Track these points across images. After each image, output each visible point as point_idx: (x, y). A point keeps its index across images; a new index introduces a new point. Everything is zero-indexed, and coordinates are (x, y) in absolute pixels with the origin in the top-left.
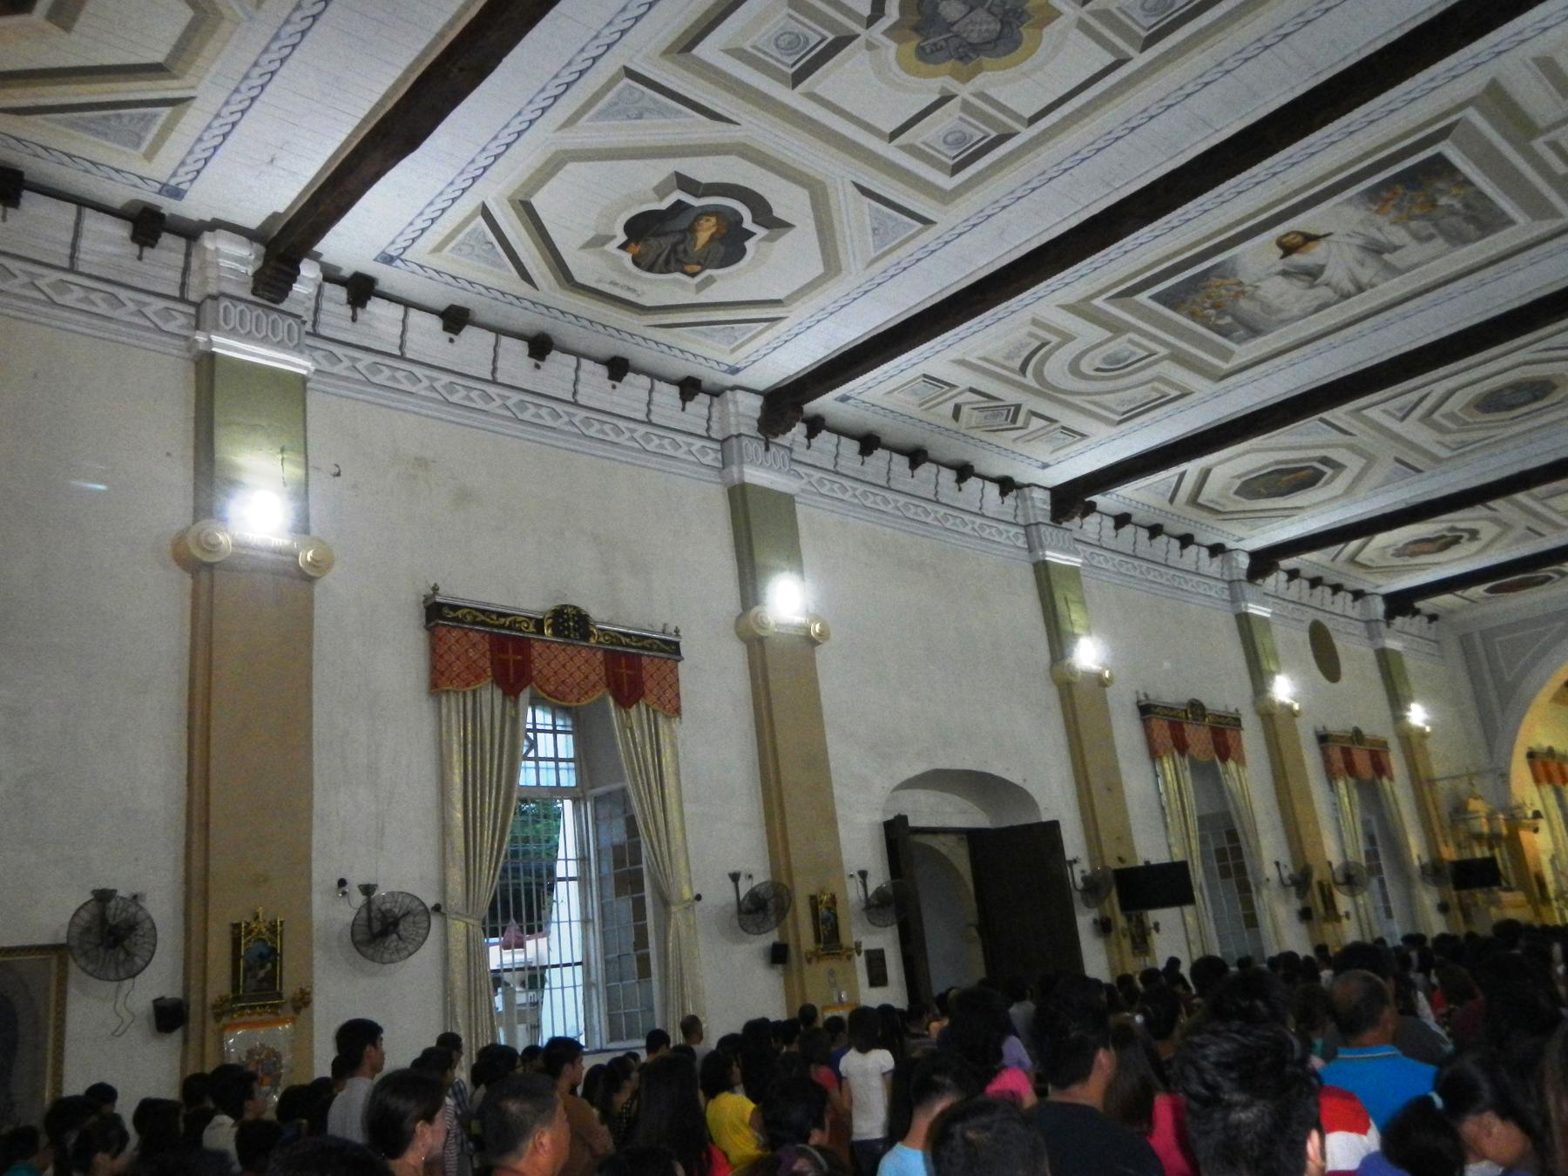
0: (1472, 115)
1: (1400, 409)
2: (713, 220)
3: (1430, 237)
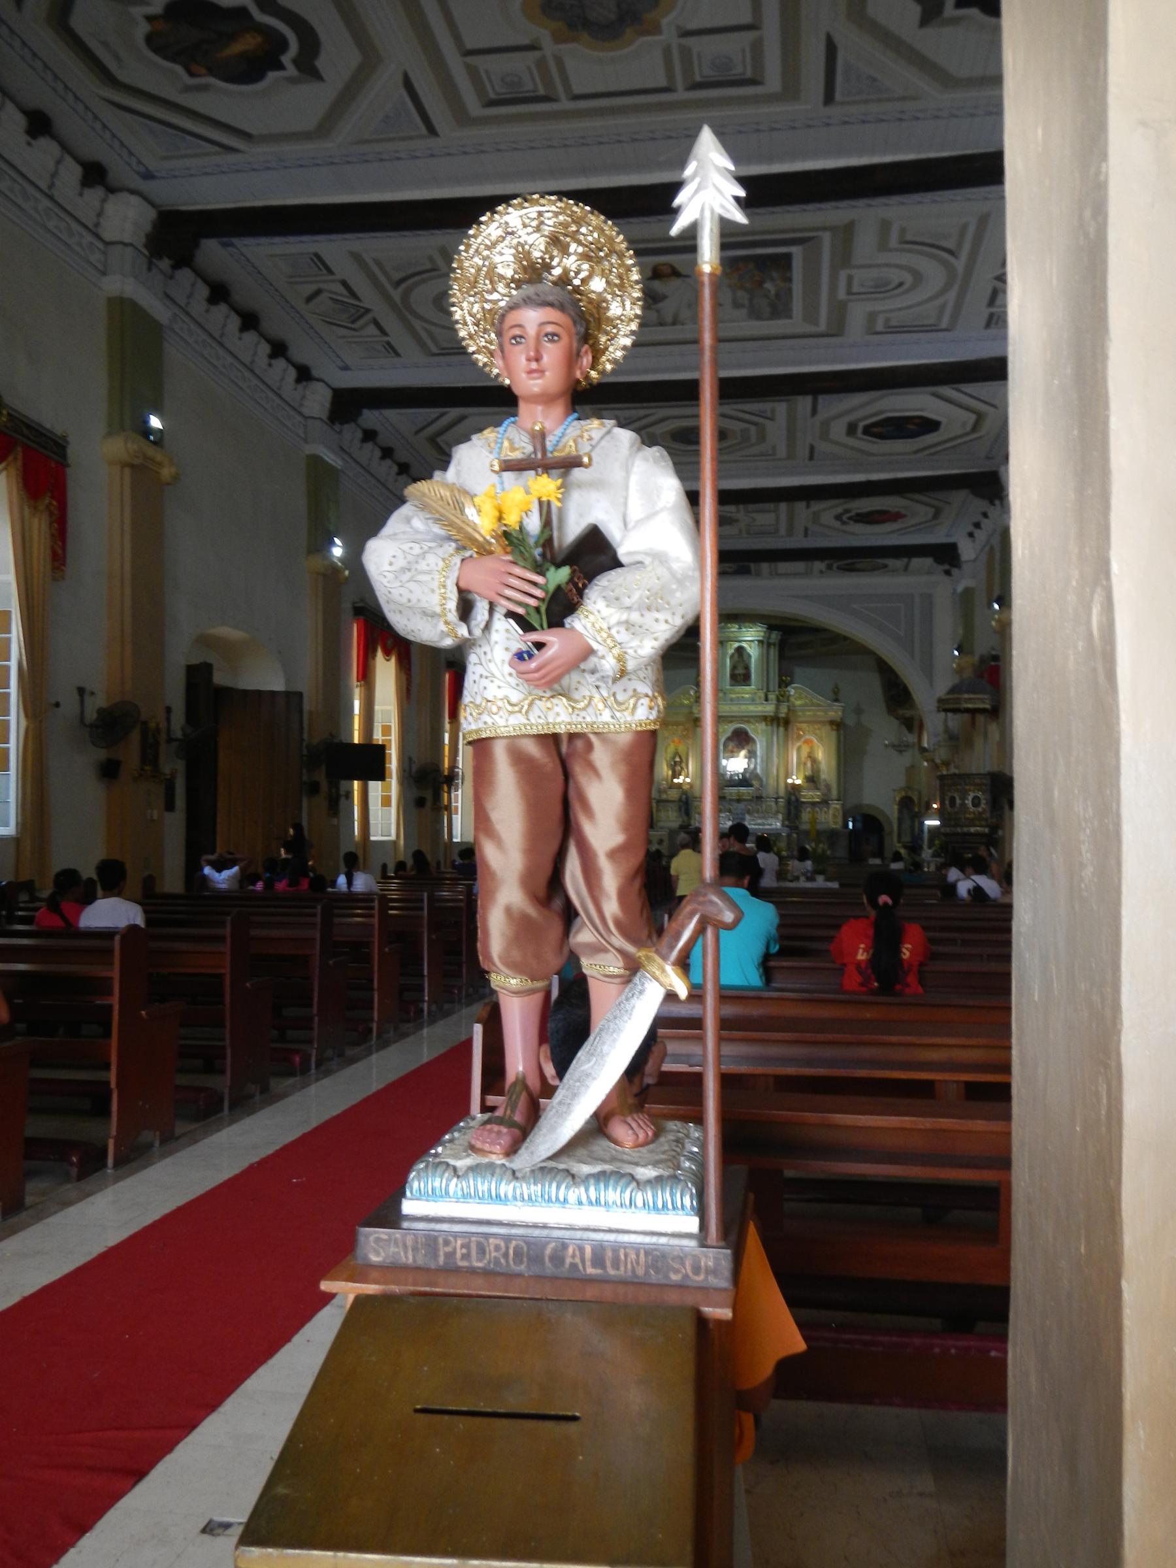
0: (826, 237)
1: (626, 419)
2: (259, 39)
3: (742, 306)
